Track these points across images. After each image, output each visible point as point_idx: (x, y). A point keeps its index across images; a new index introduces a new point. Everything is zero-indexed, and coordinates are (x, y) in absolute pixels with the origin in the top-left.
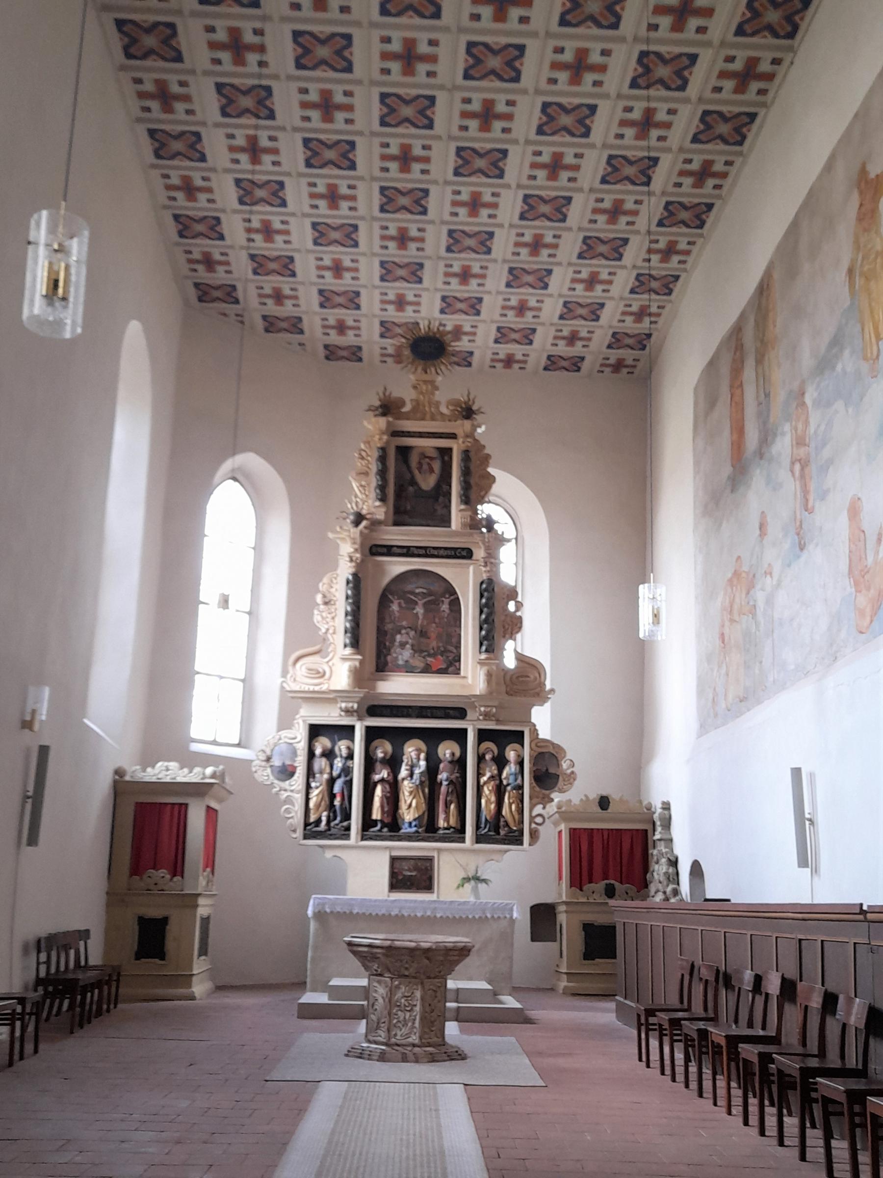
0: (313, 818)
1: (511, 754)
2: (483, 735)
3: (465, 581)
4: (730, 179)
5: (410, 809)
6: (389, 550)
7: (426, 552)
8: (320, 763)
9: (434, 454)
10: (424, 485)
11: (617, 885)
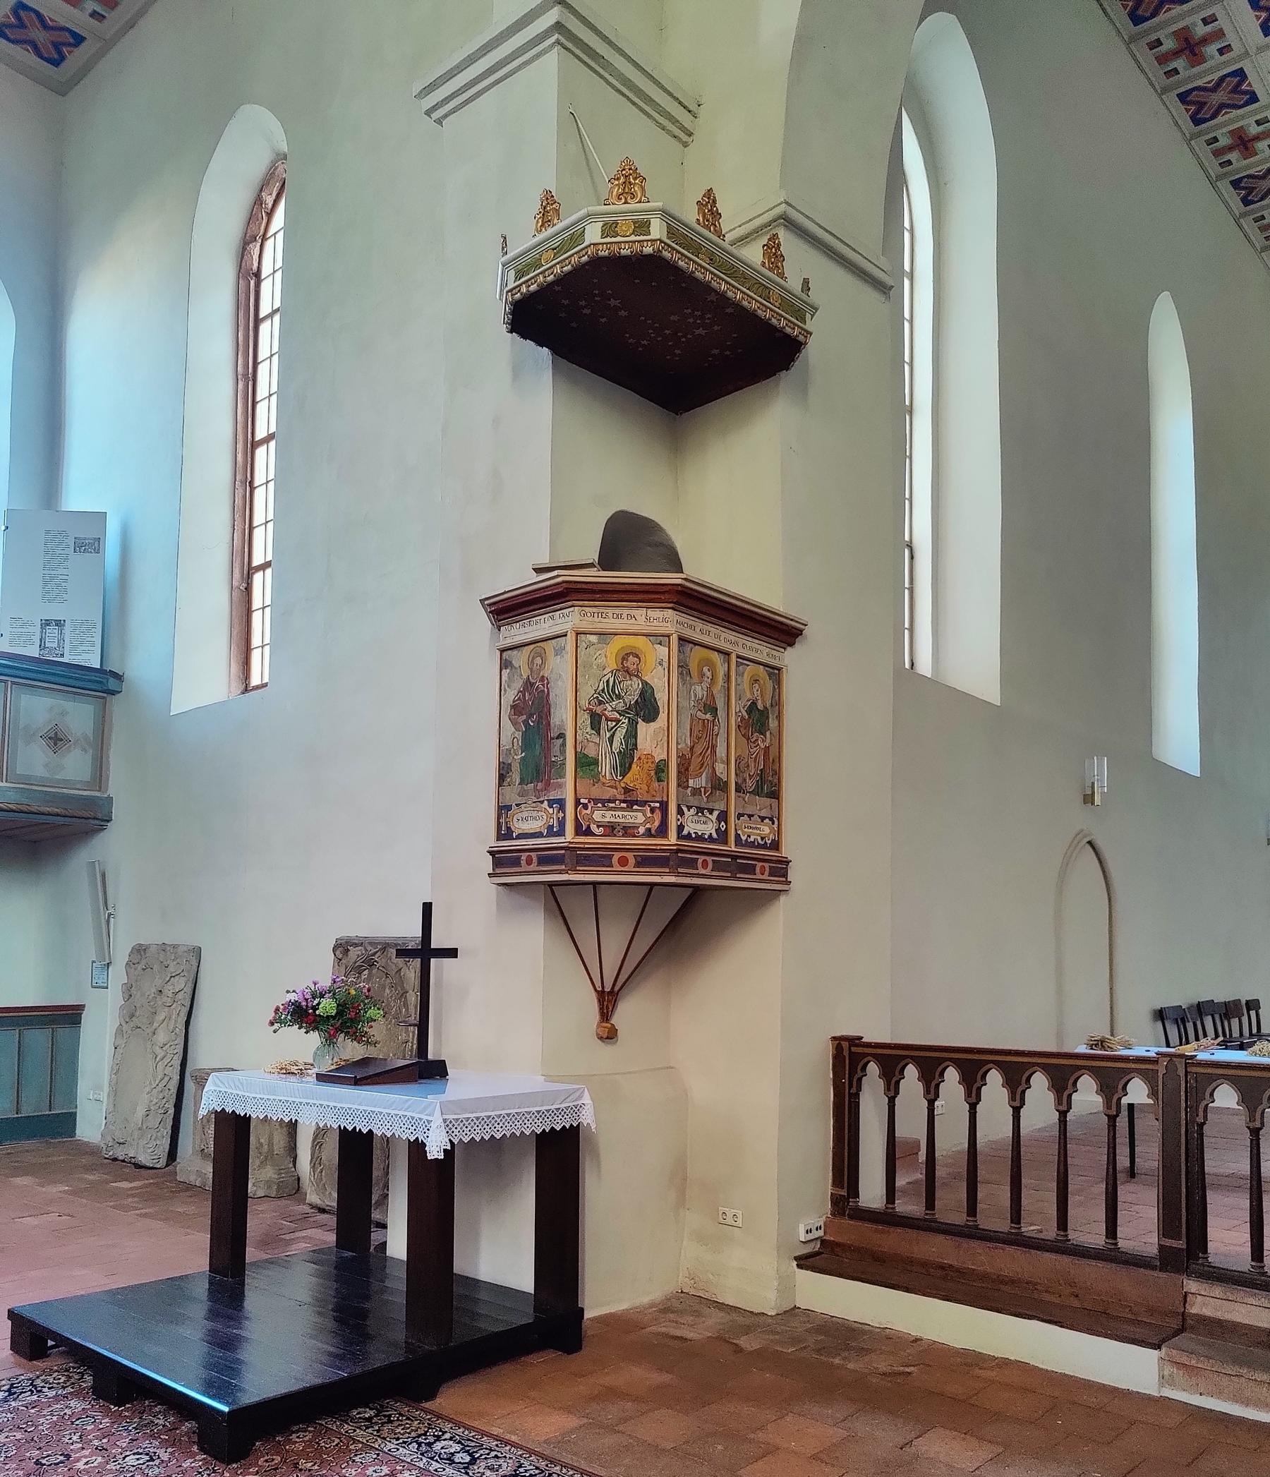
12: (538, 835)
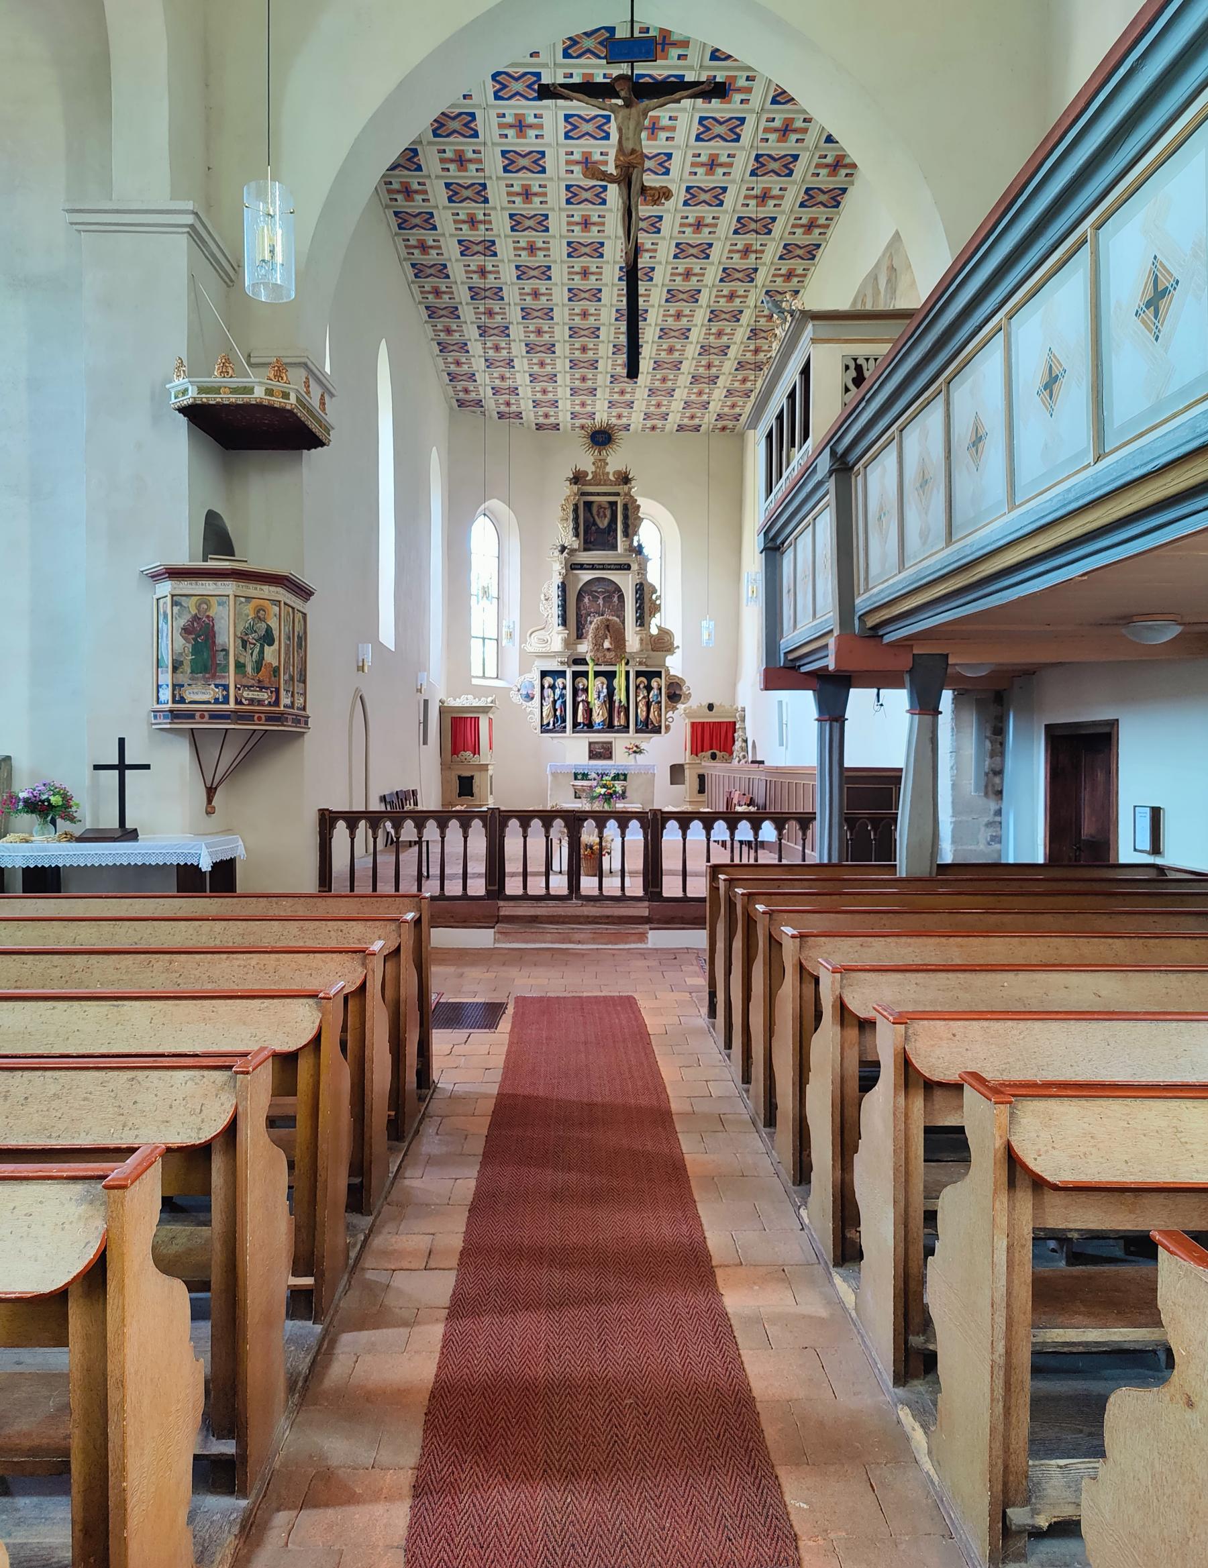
0: (545, 722)
1: (654, 684)
2: (639, 674)
3: (626, 582)
4: (831, 228)
5: (599, 717)
6: (582, 567)
7: (603, 567)
8: (548, 692)
9: (607, 506)
10: (602, 522)
11: (717, 753)
12: (208, 702)
